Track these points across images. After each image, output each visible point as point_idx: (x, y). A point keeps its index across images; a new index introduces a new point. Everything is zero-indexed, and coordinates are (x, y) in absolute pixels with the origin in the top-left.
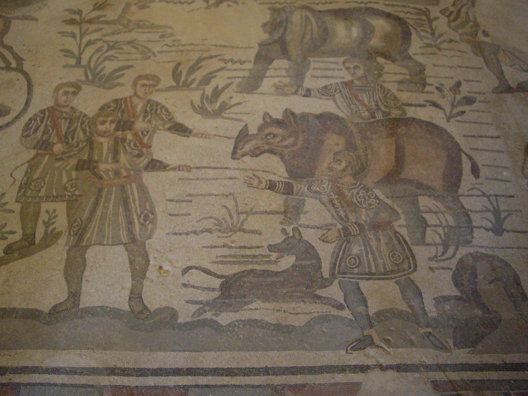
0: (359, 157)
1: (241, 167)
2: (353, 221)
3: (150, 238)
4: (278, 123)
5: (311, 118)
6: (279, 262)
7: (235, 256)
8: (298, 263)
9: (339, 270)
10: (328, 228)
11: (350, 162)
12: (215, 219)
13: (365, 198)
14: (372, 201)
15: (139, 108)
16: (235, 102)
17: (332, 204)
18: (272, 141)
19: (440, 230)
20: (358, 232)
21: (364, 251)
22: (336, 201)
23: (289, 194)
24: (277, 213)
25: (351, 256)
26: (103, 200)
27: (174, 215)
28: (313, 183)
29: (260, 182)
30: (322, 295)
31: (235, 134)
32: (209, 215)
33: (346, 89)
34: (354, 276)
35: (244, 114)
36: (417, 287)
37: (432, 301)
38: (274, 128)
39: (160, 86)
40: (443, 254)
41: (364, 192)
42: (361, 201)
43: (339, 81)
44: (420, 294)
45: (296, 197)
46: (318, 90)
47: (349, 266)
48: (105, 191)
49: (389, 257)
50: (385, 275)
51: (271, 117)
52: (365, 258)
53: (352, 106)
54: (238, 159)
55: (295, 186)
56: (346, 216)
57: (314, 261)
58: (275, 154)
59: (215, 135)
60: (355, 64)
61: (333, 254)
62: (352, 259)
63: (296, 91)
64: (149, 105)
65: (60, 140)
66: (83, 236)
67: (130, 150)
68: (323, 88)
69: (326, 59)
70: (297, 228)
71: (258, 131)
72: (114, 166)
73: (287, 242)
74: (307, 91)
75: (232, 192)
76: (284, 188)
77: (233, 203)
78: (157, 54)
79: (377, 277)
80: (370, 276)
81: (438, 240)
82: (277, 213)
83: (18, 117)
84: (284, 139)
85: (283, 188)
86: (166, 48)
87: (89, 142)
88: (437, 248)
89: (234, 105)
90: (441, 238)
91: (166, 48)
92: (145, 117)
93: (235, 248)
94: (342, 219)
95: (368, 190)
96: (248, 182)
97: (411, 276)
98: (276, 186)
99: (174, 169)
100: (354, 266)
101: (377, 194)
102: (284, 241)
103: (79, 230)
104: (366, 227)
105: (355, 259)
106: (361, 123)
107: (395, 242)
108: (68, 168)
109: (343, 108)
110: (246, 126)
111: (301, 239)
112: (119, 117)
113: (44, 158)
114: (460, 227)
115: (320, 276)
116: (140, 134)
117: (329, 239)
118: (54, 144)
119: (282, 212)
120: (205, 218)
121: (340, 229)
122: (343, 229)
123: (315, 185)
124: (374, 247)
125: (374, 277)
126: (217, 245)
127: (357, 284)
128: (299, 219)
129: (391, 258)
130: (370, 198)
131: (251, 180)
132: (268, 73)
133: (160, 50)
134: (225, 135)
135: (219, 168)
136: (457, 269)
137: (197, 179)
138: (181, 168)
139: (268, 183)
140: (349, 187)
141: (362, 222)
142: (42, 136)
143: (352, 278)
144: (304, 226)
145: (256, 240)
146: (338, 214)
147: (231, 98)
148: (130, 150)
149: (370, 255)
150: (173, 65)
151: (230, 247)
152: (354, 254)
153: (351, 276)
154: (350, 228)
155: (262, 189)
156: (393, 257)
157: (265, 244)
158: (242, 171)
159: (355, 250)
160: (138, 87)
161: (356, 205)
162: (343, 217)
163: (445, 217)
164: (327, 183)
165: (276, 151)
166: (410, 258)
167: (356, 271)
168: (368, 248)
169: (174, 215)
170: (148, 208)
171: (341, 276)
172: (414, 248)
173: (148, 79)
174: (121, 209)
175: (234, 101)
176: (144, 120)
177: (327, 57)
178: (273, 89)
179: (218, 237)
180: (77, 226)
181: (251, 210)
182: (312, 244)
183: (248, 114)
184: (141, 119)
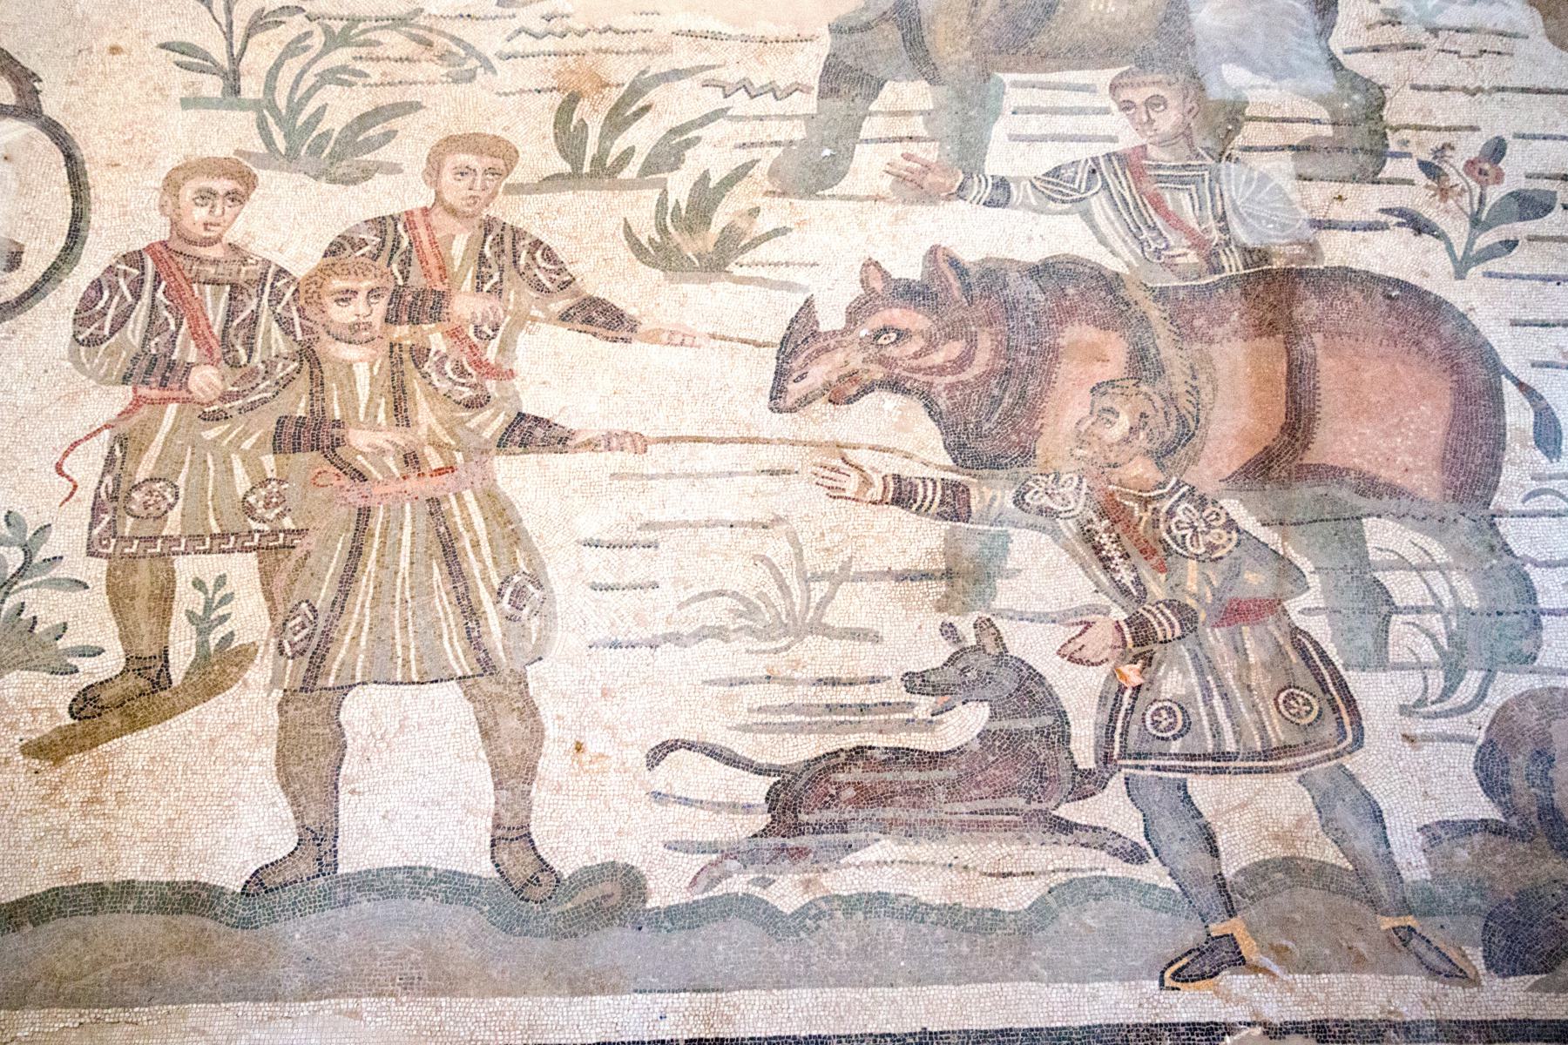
0: (1171, 399)
1: (803, 436)
2: (1161, 598)
3: (540, 659)
4: (911, 294)
5: (1013, 275)
6: (940, 722)
7: (807, 709)
8: (995, 726)
9: (1124, 747)
10: (1084, 619)
11: (1143, 415)
12: (734, 594)
13: (1195, 529)
14: (1217, 535)
16: (769, 228)
17: (1094, 548)
18: (893, 351)
19: (1435, 623)
20: (1178, 632)
21: (1197, 689)
22: (1104, 536)
23: (957, 517)
24: (926, 576)
25: (1160, 705)
26: (376, 545)
27: (608, 588)
28: (1030, 483)
29: (867, 482)
30: (1074, 819)
31: (776, 332)
32: (716, 587)
33: (1122, 179)
34: (1173, 763)
35: (800, 264)
36: (1366, 795)
37: (1415, 838)
38: (896, 312)
40: (1447, 692)
41: (1191, 507)
42: (1184, 536)
43: (1099, 149)
44: (1378, 816)
45: (980, 527)
46: (1032, 184)
47: (1154, 732)
49: (1277, 704)
50: (1269, 758)
51: (885, 276)
52: (1202, 710)
53: (1146, 234)
54: (791, 410)
55: (973, 491)
56: (1138, 581)
57: (1048, 720)
58: (907, 392)
59: (713, 336)
60: (1151, 91)
61: (1103, 698)
62: (1163, 712)
63: (961, 188)
64: (490, 238)
65: (209, 358)
67: (444, 386)
68: (1047, 174)
69: (1054, 77)
70: (989, 620)
71: (848, 321)
72: (400, 437)
73: (961, 666)
74: (996, 186)
75: (781, 513)
76: (942, 503)
77: (786, 547)
79: (1239, 764)
80: (1219, 762)
81: (1428, 653)
82: (926, 576)
83: (52, 275)
84: (932, 345)
85: (937, 500)
88: (1425, 678)
89: (767, 237)
90: (1438, 647)
93: (804, 682)
94: (1125, 592)
95: (1202, 502)
96: (830, 483)
97: (1349, 763)
98: (916, 493)
99: (591, 445)
100: (1169, 734)
101: (1233, 516)
102: (952, 660)
104: (1202, 616)
105: (1170, 711)
106: (1175, 288)
107: (1294, 661)
108: (247, 445)
109: (1118, 245)
110: (808, 303)
111: (1002, 657)
113: (163, 413)
114: (1499, 614)
115: (1067, 764)
117: (1087, 654)
119: (939, 574)
120: (703, 596)
121: (1123, 624)
122: (1129, 623)
123: (1037, 488)
124: (1229, 675)
125: (1232, 764)
126: (747, 675)
127: (1183, 787)
128: (993, 596)
129: (1282, 707)
130: (1209, 526)
131: (844, 478)
132: (870, 128)
134: (743, 335)
135: (732, 441)
136: (1490, 741)
137: (670, 475)
138: (614, 443)
139: (891, 486)
140: (1144, 495)
141: (1191, 602)
142: (146, 340)
143: (1164, 769)
144: (1011, 614)
145: (864, 660)
146: (1113, 578)
147: (755, 212)
149: (1217, 701)
150: (557, 99)
151: (791, 682)
152: (1168, 697)
153: (1161, 763)
154: (1152, 619)
155: (874, 503)
156: (1288, 707)
157: (893, 671)
158: (807, 449)
159: (1174, 682)
161: (1167, 548)
162: (1129, 584)
163: (1449, 582)
164: (1075, 484)
165: (908, 385)
166: (1342, 707)
167: (1175, 747)
168: (1209, 678)
169: (608, 588)
170: (522, 565)
171: (1130, 762)
172: (1351, 677)
175: (764, 224)
177: (1059, 69)
178: (889, 179)
179: (747, 651)
181: (844, 568)
182: (1039, 670)
183: (814, 264)
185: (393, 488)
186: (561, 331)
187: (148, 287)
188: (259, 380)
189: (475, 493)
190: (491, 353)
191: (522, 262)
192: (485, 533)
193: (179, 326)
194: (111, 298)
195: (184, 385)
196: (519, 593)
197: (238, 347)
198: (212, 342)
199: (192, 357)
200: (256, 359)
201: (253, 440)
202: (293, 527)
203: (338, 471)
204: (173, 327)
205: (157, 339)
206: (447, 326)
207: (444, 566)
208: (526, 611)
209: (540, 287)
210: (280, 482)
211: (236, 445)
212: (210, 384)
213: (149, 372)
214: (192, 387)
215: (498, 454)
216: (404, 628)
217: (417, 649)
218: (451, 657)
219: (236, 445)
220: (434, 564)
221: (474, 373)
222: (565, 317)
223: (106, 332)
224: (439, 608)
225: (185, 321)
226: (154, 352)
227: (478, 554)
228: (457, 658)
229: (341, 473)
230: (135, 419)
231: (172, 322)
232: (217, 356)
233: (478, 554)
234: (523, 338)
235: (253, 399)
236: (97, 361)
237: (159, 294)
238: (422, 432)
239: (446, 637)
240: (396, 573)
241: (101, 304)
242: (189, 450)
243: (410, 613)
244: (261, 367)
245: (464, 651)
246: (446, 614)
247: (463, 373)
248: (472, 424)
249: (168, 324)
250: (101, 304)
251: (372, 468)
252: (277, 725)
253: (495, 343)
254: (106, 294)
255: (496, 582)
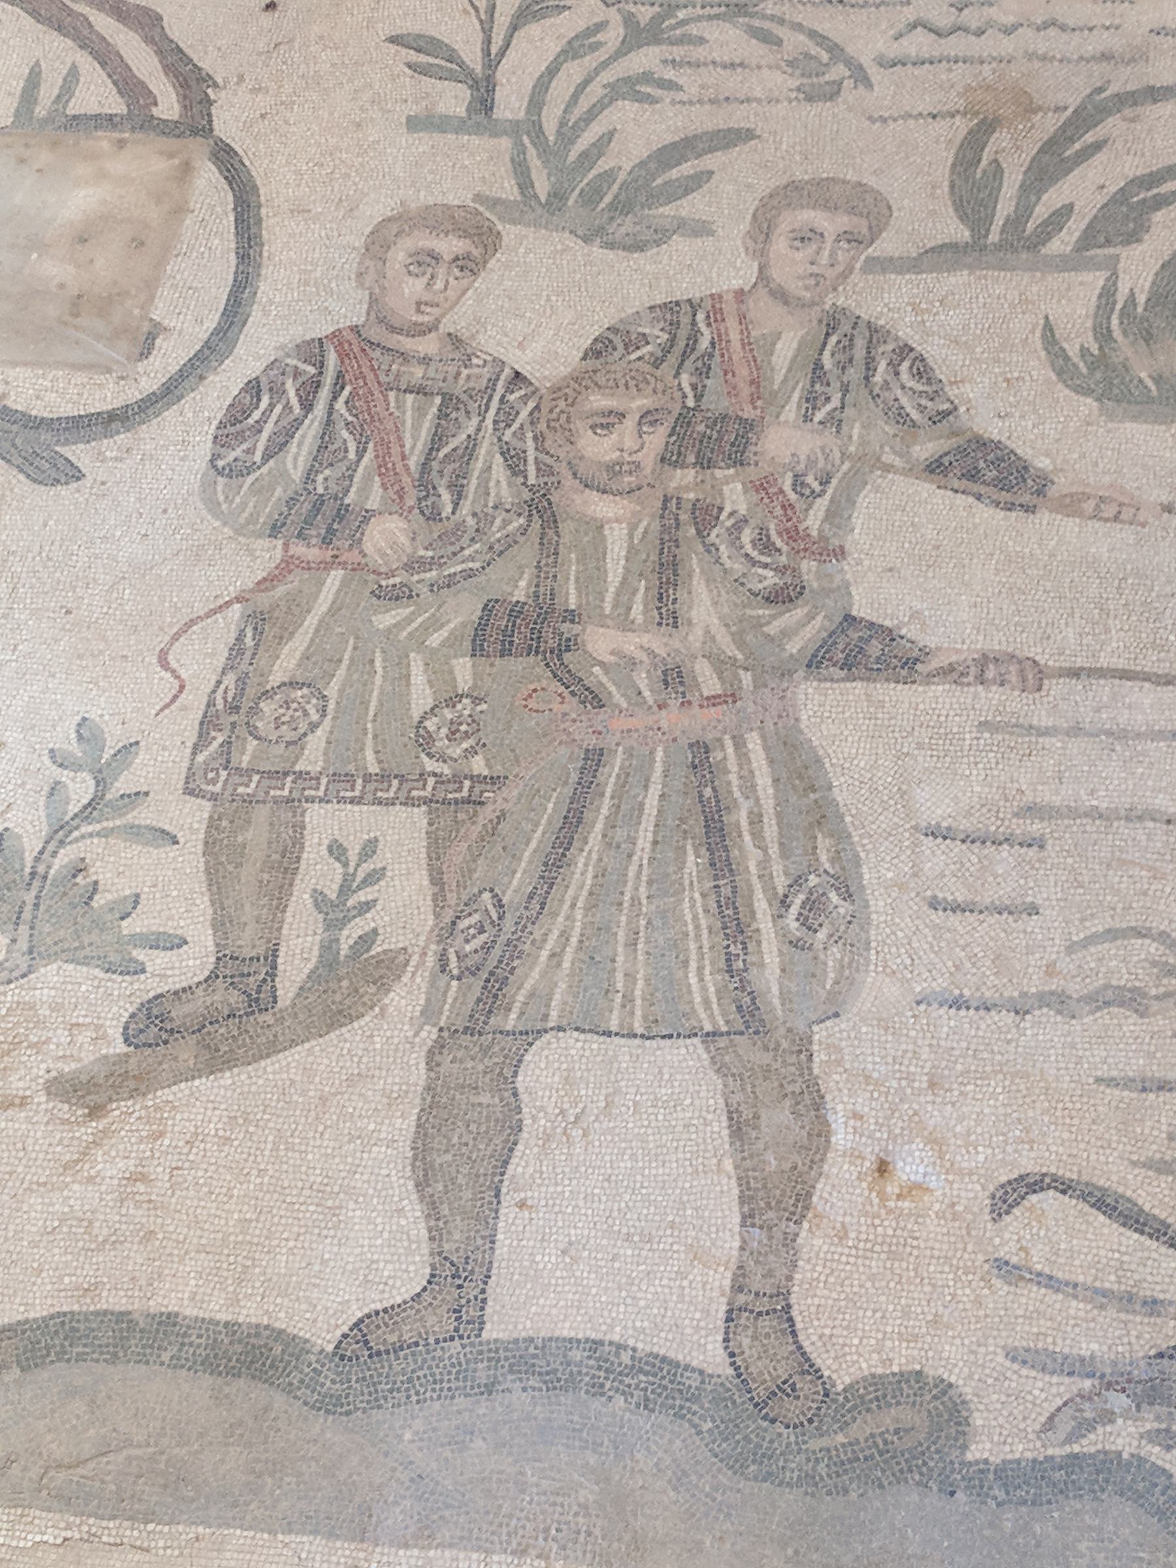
15: (785, 351)
26: (605, 811)
39: (887, 245)
48: (616, 763)
64: (833, 339)
66: (505, 981)
78: (873, 71)
86: (919, 44)
87: (536, 517)
91: (919, 44)
92: (812, 401)
103: (487, 948)
112: (685, 396)
116: (787, 487)
118: (367, 516)
133: (894, 50)
148: (738, 567)
150: (962, 126)
160: (780, 245)
173: (829, 206)
174: (691, 858)
176: (807, 418)
180: (482, 931)
184: (791, 412)
185: (640, 721)
186: (925, 489)
187: (324, 394)
188: (465, 541)
189: (764, 738)
190: (814, 521)
191: (878, 379)
192: (771, 802)
193: (360, 454)
194: (272, 406)
195: (356, 542)
196: (815, 904)
197: (442, 490)
198: (406, 480)
199: (374, 502)
200: (465, 509)
201: (444, 633)
202: (486, 772)
203: (562, 689)
204: (352, 455)
205: (327, 472)
206: (752, 473)
207: (703, 851)
208: (821, 935)
209: (902, 417)
210: (477, 701)
211: (419, 640)
212: (393, 545)
213: (308, 522)
214: (368, 546)
215: (806, 679)
216: (632, 944)
217: (647, 980)
218: (698, 999)
219: (419, 640)
220: (689, 847)
221: (785, 548)
222: (936, 468)
223: (258, 457)
224: (689, 917)
225: (371, 446)
226: (320, 490)
227: (757, 835)
228: (706, 1002)
229: (566, 693)
230: (281, 590)
231: (352, 446)
232: (410, 502)
233: (757, 835)
234: (866, 499)
235: (452, 570)
236: (238, 500)
237: (340, 405)
238: (696, 637)
239: (693, 965)
240: (630, 856)
241: (256, 415)
242: (351, 642)
243: (643, 923)
244: (471, 522)
245: (718, 991)
246: (697, 927)
247: (766, 545)
248: (772, 629)
249: (346, 451)
250: (256, 415)
251: (613, 689)
252: (422, 1083)
253: (822, 504)
254: (265, 401)
255: (781, 883)
